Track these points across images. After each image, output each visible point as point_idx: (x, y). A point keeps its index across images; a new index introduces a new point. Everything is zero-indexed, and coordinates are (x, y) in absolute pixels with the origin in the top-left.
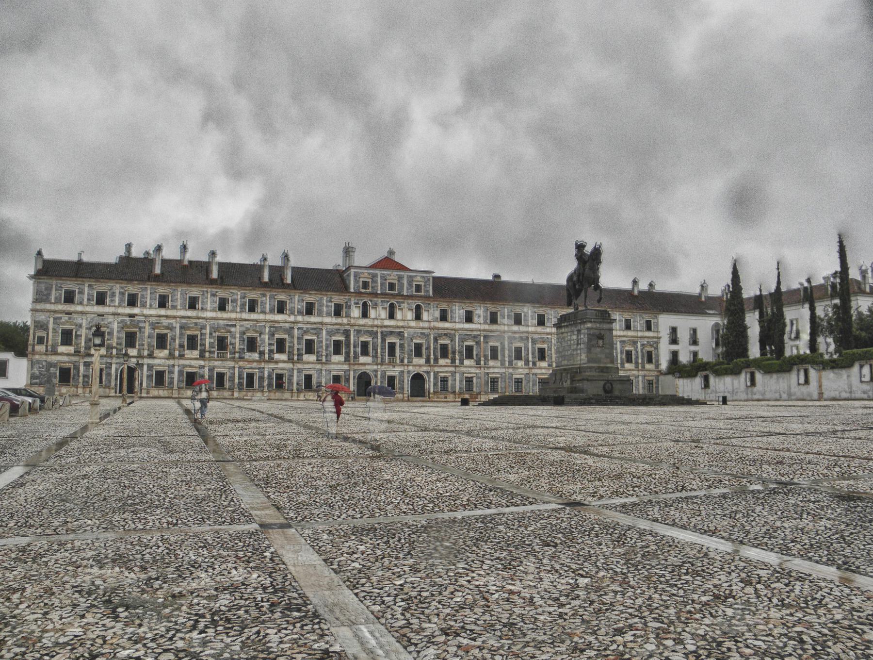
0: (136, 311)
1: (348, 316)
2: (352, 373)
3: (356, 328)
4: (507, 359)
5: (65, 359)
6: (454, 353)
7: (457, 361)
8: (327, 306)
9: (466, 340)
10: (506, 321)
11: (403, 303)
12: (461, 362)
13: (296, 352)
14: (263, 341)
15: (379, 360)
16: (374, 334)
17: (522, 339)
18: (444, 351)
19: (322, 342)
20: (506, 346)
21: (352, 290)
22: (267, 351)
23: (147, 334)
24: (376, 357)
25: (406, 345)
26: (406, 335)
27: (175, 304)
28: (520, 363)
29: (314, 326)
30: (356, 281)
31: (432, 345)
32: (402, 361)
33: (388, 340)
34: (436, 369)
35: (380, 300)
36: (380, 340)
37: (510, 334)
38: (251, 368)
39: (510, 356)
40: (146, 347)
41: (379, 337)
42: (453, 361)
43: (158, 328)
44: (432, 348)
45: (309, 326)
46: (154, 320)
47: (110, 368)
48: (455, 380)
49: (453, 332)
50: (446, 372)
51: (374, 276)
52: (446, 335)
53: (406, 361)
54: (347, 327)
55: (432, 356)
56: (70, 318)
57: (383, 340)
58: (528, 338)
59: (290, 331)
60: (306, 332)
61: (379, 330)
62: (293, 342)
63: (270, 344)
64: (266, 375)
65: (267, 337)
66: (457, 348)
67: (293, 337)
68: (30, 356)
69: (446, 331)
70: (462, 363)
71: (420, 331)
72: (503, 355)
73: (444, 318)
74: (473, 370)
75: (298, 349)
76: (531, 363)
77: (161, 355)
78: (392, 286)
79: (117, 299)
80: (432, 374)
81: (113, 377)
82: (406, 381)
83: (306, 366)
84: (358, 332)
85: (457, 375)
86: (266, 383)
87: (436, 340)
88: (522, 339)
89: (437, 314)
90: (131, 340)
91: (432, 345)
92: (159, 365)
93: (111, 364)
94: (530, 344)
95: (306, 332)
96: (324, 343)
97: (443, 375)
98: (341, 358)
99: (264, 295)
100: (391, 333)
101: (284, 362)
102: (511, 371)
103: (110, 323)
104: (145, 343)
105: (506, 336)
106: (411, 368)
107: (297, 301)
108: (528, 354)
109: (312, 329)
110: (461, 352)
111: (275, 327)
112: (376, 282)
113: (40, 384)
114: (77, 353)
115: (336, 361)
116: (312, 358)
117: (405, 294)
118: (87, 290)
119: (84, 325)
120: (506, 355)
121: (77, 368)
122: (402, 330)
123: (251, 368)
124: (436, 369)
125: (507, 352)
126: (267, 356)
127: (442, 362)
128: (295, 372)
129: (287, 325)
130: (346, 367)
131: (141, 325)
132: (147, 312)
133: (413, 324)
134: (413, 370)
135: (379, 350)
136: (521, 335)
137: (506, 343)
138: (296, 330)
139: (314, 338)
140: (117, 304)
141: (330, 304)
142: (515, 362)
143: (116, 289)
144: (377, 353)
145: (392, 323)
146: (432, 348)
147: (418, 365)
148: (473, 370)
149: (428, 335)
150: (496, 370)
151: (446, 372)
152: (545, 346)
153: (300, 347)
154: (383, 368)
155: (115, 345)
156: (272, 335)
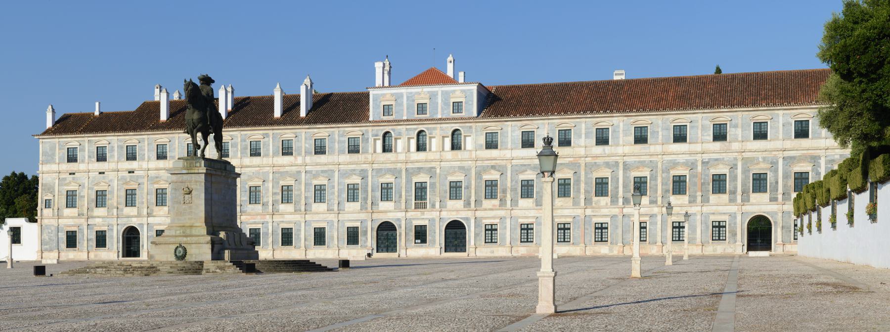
0: (133, 165)
1: (366, 152)
2: (369, 224)
3: (375, 166)
4: (582, 197)
5: (70, 222)
6: (504, 191)
7: (509, 202)
8: (339, 142)
9: (523, 172)
10: (582, 141)
11: (435, 129)
12: (514, 202)
13: (303, 202)
14: (268, 190)
15: (403, 206)
16: (396, 173)
17: (607, 165)
18: (491, 190)
19: (333, 187)
20: (583, 178)
21: (371, 119)
22: (271, 203)
23: (146, 191)
24: (400, 202)
25: (438, 185)
26: (438, 171)
27: (173, 155)
28: (604, 201)
29: (325, 168)
30: (376, 106)
31: (473, 182)
32: (433, 206)
33: (416, 179)
34: (479, 214)
35: (404, 127)
36: (404, 181)
37: (588, 160)
38: (255, 223)
39: (586, 192)
40: (145, 205)
41: (404, 176)
42: (503, 202)
43: (157, 183)
44: (473, 187)
45: (319, 168)
46: (152, 173)
47: (112, 230)
48: (505, 228)
49: (503, 163)
50: (494, 218)
51: (398, 98)
52: (493, 167)
53: (437, 205)
54: (364, 166)
55: (473, 199)
56: (73, 179)
57: (408, 181)
58: (617, 163)
59: (296, 177)
60: (316, 176)
61: (403, 167)
62: (300, 190)
63: (274, 194)
64: (270, 231)
65: (270, 185)
66: (509, 185)
67: (300, 183)
68: (39, 221)
69: (493, 163)
70: (517, 205)
71: (458, 164)
72: (579, 191)
73: (491, 144)
74: (533, 213)
75: (306, 198)
76: (621, 200)
77: (161, 213)
78: (421, 108)
79: (116, 154)
80: (473, 221)
81: (115, 240)
82: (437, 231)
83: (316, 217)
84: (379, 171)
85: (508, 221)
86: (270, 240)
87: (479, 175)
88: (607, 165)
89: (482, 141)
90: (130, 198)
91: (473, 182)
92: (160, 224)
93: (113, 226)
94: (621, 173)
95: (316, 176)
96: (336, 189)
97: (488, 222)
98: (356, 206)
99: (267, 135)
100: (420, 170)
101: (291, 214)
102: (589, 212)
103: (111, 181)
104: (145, 200)
105: (582, 162)
106: (444, 214)
107: (303, 136)
108: (617, 188)
109: (323, 171)
110: (513, 190)
111: (281, 173)
112: (401, 104)
113: (51, 250)
114: (80, 215)
115: (351, 210)
116: (322, 207)
117: (439, 116)
118: (85, 144)
119: (86, 185)
120: (582, 191)
121: (82, 230)
122: (433, 164)
123: (255, 223)
124: (479, 214)
125: (583, 186)
126: (271, 207)
127: (488, 204)
128: (303, 224)
129: (294, 169)
130: (363, 216)
131: (140, 181)
132: (145, 165)
133: (449, 154)
134: (450, 216)
135: (403, 194)
136: (607, 159)
137: (583, 173)
138: (303, 174)
139: (325, 182)
140: (116, 159)
141: (342, 139)
142: (595, 199)
143: (115, 142)
144: (401, 196)
145: (422, 155)
146: (473, 187)
147: (455, 211)
148: (533, 213)
149: (469, 169)
150: (566, 212)
151: (494, 218)
152: (645, 173)
153: (308, 194)
154: (409, 215)
155: (115, 204)
156: (275, 182)
